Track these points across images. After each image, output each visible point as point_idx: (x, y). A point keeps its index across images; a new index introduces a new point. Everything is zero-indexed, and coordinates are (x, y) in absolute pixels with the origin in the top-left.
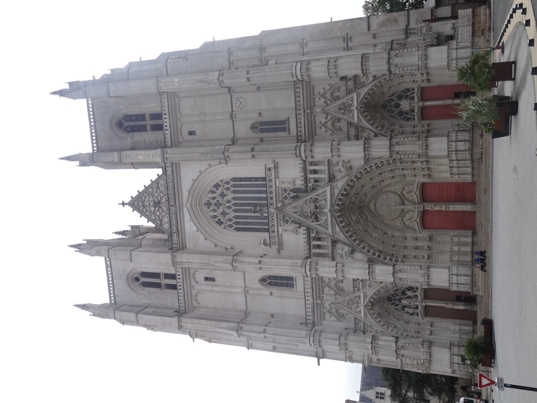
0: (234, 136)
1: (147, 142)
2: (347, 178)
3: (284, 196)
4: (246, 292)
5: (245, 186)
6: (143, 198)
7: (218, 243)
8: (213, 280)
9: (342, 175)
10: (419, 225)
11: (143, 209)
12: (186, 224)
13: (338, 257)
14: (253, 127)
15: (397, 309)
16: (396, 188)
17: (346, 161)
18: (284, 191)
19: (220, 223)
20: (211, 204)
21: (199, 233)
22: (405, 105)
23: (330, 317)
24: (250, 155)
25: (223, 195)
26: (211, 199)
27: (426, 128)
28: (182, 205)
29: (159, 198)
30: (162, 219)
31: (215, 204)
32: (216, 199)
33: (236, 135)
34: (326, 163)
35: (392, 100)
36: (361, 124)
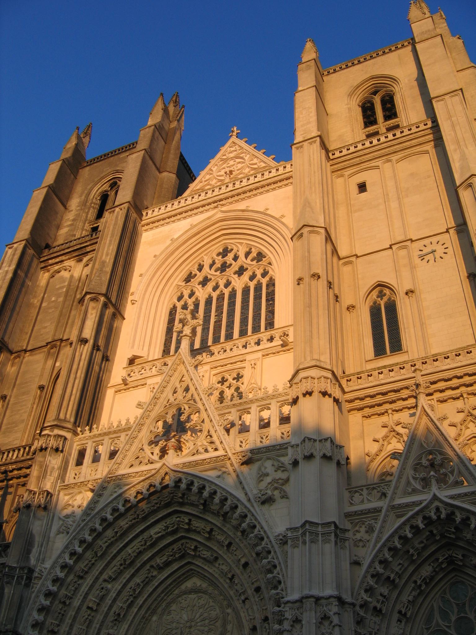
3: (227, 376)
17: (286, 488)
19: (189, 278)
33: (360, 259)
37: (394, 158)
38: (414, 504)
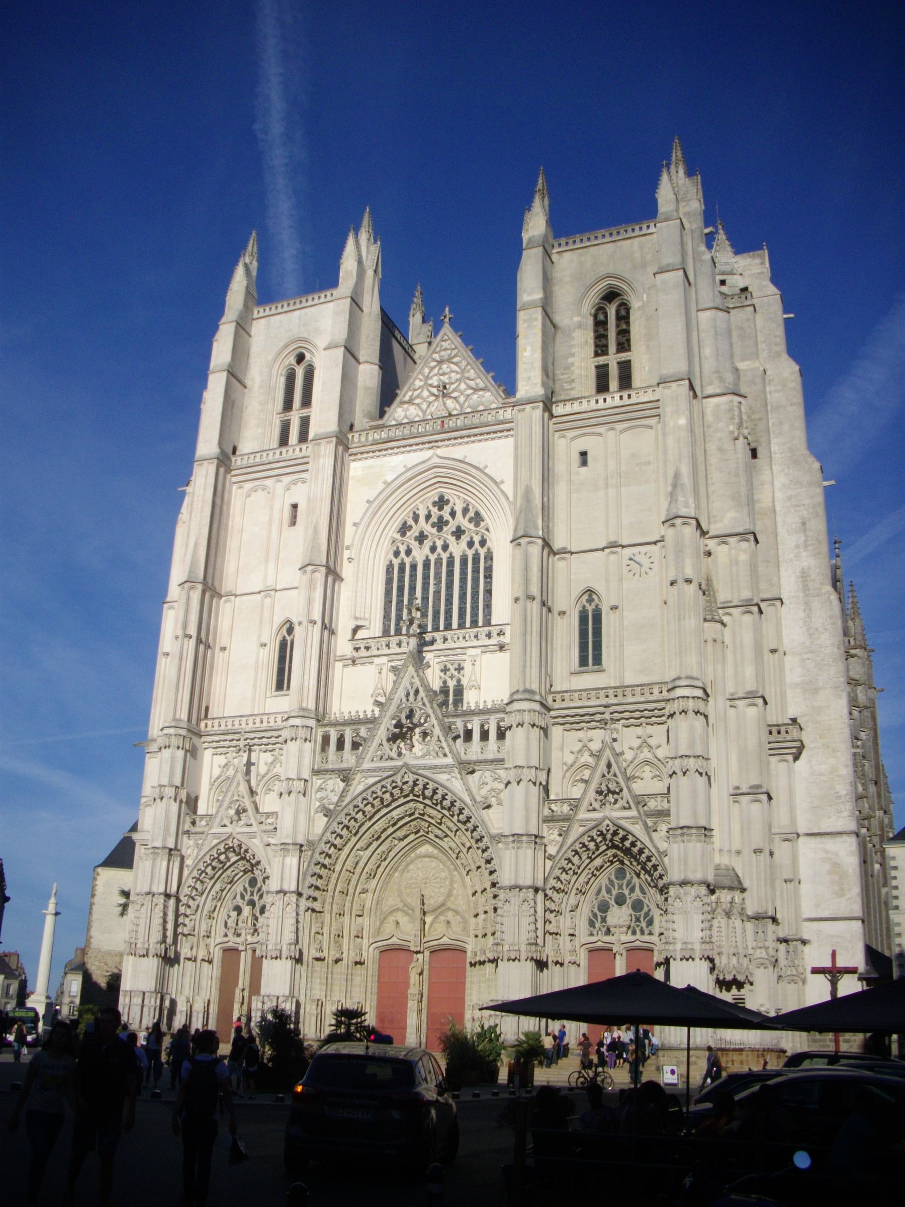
0: (572, 553)
1: (570, 360)
2: (467, 800)
3: (449, 666)
4: (268, 591)
5: (476, 580)
6: (456, 360)
7: (361, 528)
8: (293, 523)
9: (475, 791)
10: (385, 943)
11: (436, 361)
12: (401, 457)
13: (320, 782)
14: (590, 592)
15: (235, 898)
16: (460, 897)
18: (459, 665)
19: (404, 529)
20: (441, 508)
21: (381, 486)
22: (619, 916)
23: (219, 766)
24: (520, 593)
25: (458, 533)
27: (568, 958)
28: (438, 447)
29: (455, 395)
30: (414, 404)
31: (440, 518)
32: (450, 519)
33: (574, 556)
34: (499, 756)
35: (632, 890)
36: (576, 825)
37: (620, 427)
38: (592, 820)
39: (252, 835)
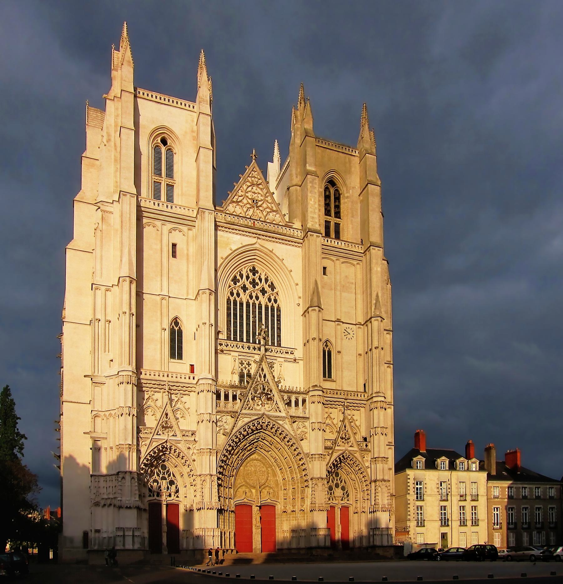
5: (273, 321)
20: (254, 275)
22: (338, 492)
26: (260, 277)
31: (254, 280)
32: (259, 283)
37: (342, 260)
39: (178, 442)
